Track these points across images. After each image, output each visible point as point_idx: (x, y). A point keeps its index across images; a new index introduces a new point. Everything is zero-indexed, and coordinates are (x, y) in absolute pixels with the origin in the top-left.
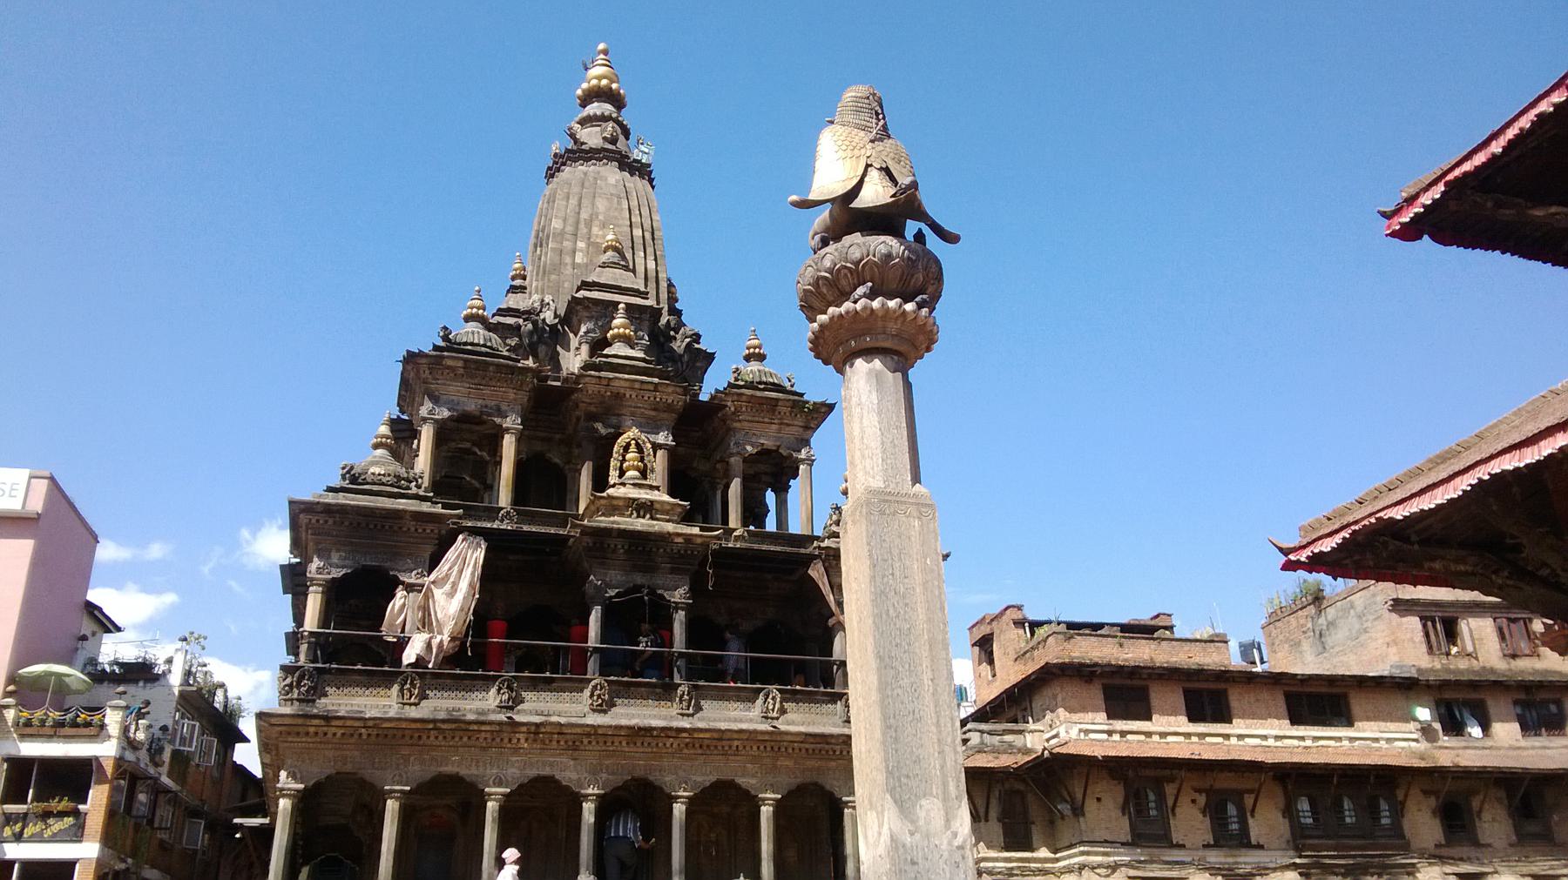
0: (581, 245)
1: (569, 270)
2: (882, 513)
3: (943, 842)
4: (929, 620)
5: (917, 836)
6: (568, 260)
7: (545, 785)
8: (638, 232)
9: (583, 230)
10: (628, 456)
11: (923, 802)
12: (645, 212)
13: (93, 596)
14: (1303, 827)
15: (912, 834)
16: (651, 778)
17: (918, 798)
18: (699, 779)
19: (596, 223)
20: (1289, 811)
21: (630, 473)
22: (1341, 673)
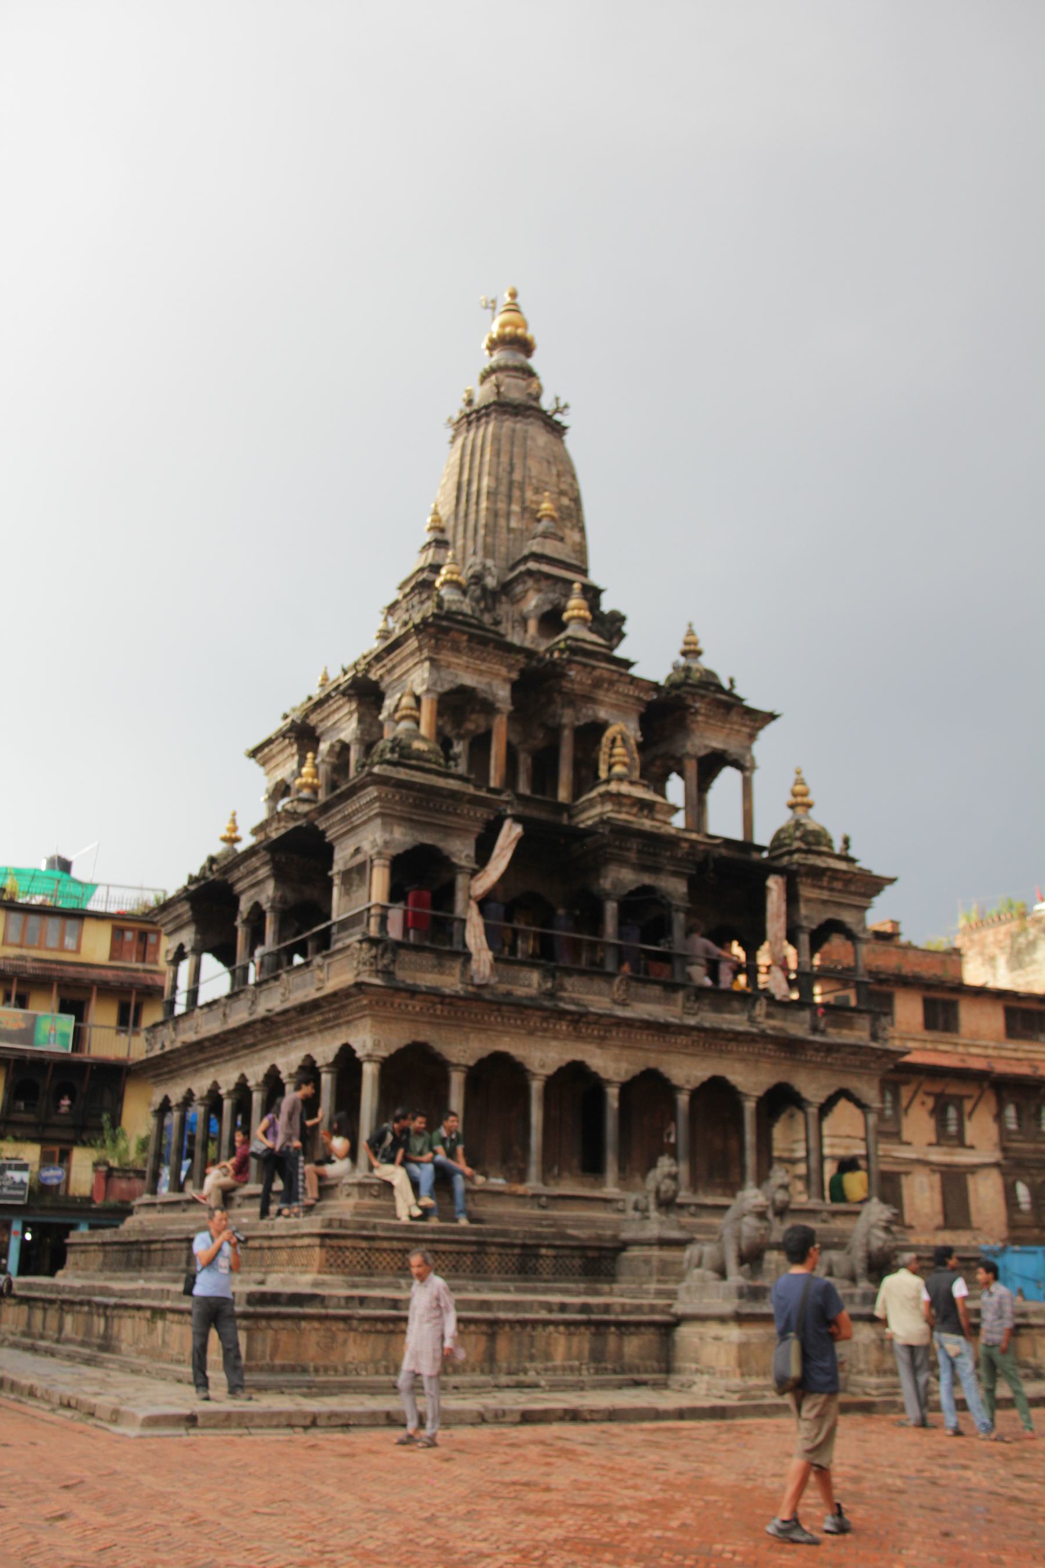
0: (516, 508)
1: (503, 534)
6: (502, 522)
7: (576, 1071)
9: (516, 493)
14: (1010, 1132)
16: (663, 1069)
20: (999, 1117)
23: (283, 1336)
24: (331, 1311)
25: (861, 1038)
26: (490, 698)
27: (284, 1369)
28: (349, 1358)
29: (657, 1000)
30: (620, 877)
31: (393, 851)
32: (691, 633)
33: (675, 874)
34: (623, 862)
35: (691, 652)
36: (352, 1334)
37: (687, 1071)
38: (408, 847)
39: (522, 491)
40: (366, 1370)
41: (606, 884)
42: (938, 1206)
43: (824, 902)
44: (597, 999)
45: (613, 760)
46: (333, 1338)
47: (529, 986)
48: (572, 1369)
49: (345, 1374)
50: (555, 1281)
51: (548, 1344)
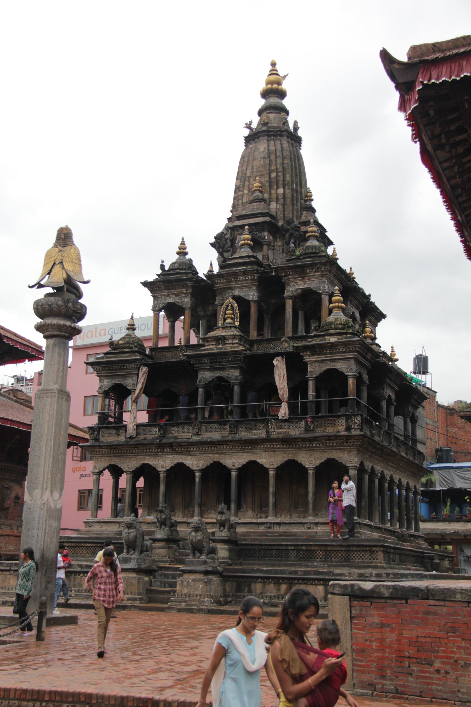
0: (246, 192)
2: (40, 398)
3: (39, 502)
4: (48, 433)
5: (32, 501)
7: (180, 467)
8: (274, 175)
9: (247, 183)
10: (227, 312)
11: (36, 491)
15: (31, 500)
16: (221, 462)
17: (35, 489)
18: (241, 461)
21: (229, 321)
22: (30, 457)
24: (3, 568)
26: (181, 305)
28: (11, 584)
29: (217, 430)
30: (206, 376)
31: (103, 390)
33: (232, 368)
34: (205, 369)
36: (12, 576)
37: (234, 461)
38: (110, 386)
39: (249, 181)
40: (15, 588)
43: (323, 361)
44: (184, 434)
45: (226, 316)
46: (6, 577)
47: (155, 434)
49: (8, 590)
51: (81, 580)
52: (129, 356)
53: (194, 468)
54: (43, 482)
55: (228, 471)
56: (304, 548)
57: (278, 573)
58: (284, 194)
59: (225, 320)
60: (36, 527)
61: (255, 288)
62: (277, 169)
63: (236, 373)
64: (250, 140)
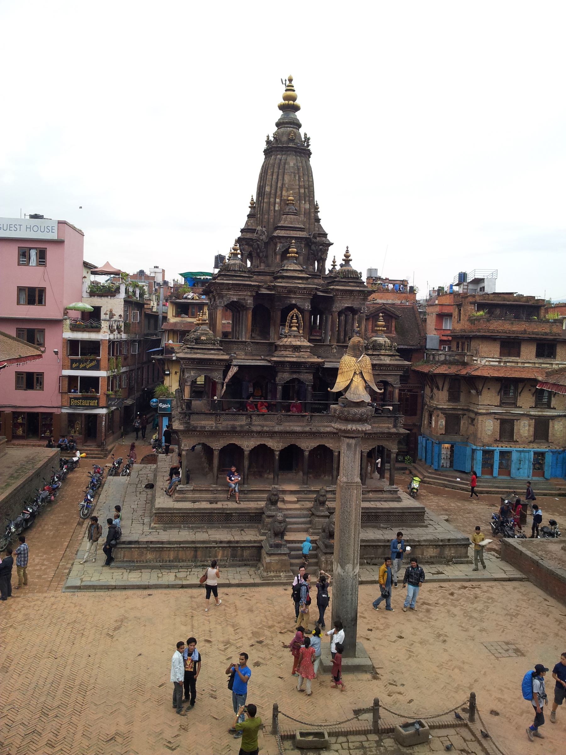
1: (272, 213)
6: (272, 208)
7: (263, 447)
8: (302, 191)
9: (279, 193)
12: (306, 178)
13: (86, 259)
19: (284, 189)
23: (126, 553)
25: (389, 428)
27: (127, 561)
30: (284, 377)
32: (347, 251)
35: (347, 260)
41: (277, 379)
42: (532, 433)
46: (143, 553)
48: (224, 560)
49: (146, 562)
50: (238, 523)
51: (216, 553)
52: (215, 354)
53: (275, 448)
54: (354, 558)
55: (301, 451)
56: (373, 514)
57: (375, 542)
58: (310, 209)
59: (291, 327)
60: (350, 593)
61: (309, 300)
62: (304, 185)
63: (311, 377)
64: (277, 151)
